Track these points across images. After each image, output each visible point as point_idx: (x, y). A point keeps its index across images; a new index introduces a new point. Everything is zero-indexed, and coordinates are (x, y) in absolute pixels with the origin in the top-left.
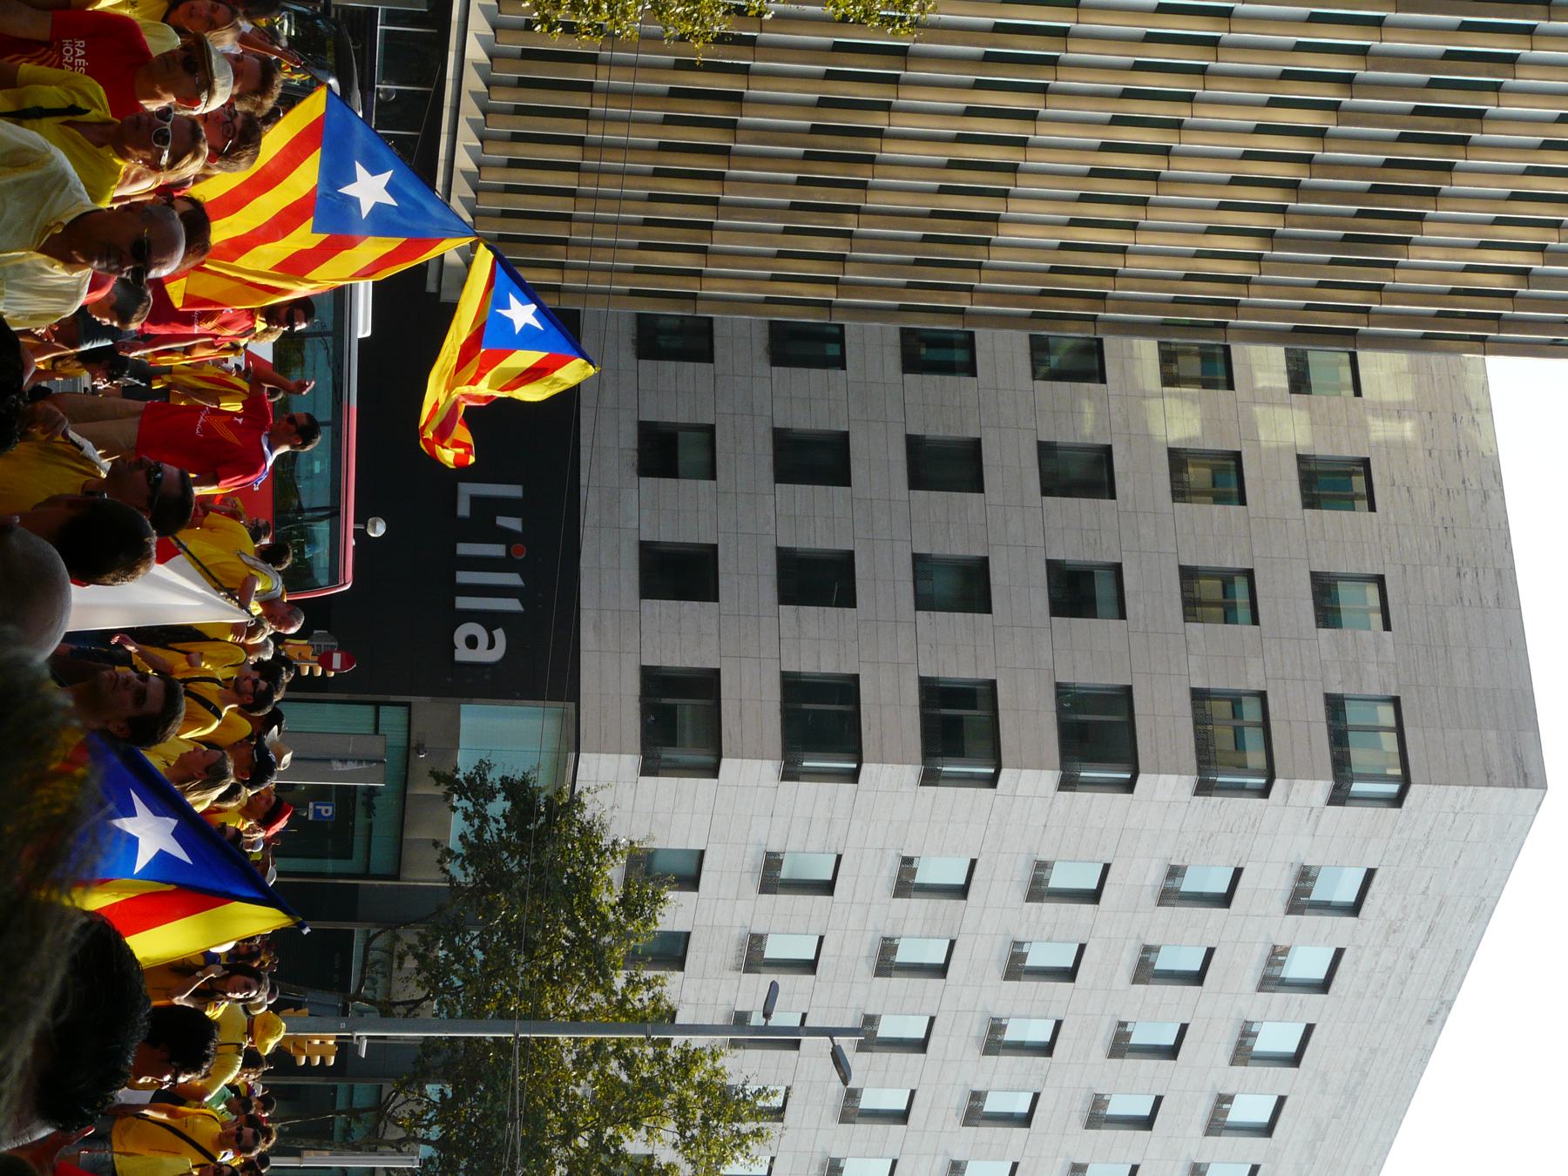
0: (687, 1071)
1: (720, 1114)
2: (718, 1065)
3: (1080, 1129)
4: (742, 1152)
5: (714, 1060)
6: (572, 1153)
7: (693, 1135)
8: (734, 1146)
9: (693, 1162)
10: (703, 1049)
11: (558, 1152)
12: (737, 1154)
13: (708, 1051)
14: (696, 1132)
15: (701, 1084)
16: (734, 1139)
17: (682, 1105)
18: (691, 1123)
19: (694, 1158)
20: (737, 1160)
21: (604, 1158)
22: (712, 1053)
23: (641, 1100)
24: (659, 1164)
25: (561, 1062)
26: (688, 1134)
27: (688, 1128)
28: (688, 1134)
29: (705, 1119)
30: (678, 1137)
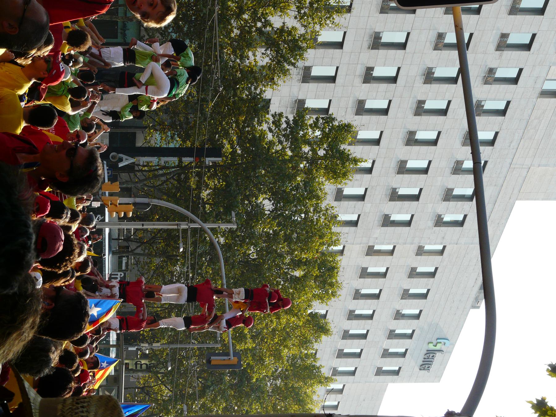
6: (242, 23)
7: (305, 12)
8: (326, 18)
9: (305, 26)
11: (234, 23)
12: (328, 22)
14: (306, 10)
16: (326, 14)
18: (304, 6)
19: (305, 24)
20: (328, 25)
21: (259, 24)
24: (288, 28)
26: (302, 12)
27: (302, 8)
30: (297, 13)
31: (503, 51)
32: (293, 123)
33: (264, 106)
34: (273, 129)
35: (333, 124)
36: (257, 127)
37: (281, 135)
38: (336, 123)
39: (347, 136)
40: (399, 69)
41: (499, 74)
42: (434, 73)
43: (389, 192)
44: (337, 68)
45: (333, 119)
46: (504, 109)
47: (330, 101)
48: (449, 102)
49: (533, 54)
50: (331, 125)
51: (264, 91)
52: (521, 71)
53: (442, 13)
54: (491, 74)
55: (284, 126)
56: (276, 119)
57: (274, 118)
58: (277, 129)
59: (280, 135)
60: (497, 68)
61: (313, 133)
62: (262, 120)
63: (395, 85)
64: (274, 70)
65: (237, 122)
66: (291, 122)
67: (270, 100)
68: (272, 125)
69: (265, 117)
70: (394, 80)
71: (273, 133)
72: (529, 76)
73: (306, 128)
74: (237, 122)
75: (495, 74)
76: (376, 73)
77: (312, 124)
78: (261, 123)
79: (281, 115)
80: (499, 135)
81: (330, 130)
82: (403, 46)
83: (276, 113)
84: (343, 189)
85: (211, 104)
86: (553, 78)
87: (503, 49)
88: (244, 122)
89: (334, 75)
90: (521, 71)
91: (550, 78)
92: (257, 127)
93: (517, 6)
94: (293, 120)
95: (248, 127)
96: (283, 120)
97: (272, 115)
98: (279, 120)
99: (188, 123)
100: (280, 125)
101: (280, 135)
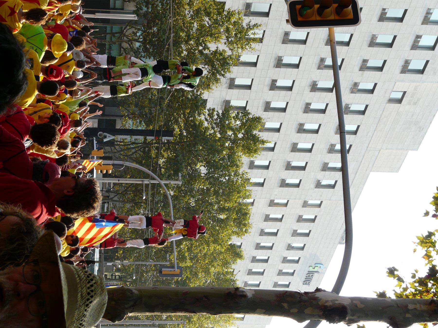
0: (230, 18)
1: (241, 32)
2: (240, 16)
3: (367, 47)
4: (249, 46)
5: (239, 15)
6: (189, 47)
8: (246, 44)
9: (232, 50)
10: (235, 11)
13: (237, 12)
15: (235, 22)
17: (227, 30)
18: (231, 36)
21: (201, 48)
22: (238, 12)
23: (214, 27)
24: (220, 51)
25: (185, 15)
26: (230, 40)
28: (230, 40)
29: (236, 35)
31: (364, 71)
32: (221, 115)
33: (202, 103)
34: (208, 119)
35: (248, 117)
36: (198, 117)
37: (214, 123)
38: (251, 116)
39: (258, 125)
40: (294, 81)
41: (361, 87)
42: (317, 85)
43: (285, 164)
44: (253, 80)
45: (249, 113)
46: (364, 110)
47: (247, 102)
48: (327, 105)
49: (384, 73)
50: (247, 117)
51: (203, 93)
52: (376, 84)
53: (324, 45)
54: (356, 86)
55: (216, 117)
56: (210, 112)
57: (209, 112)
58: (211, 119)
59: (213, 123)
60: (360, 83)
61: (235, 122)
62: (201, 113)
63: (291, 92)
64: (210, 79)
65: (184, 114)
66: (221, 115)
67: (207, 100)
68: (207, 116)
69: (203, 111)
70: (290, 89)
71: (208, 122)
72: (381, 89)
73: (230, 119)
74: (184, 114)
75: (358, 86)
76: (278, 84)
77: (234, 116)
78: (200, 115)
79: (213, 110)
80: (360, 128)
81: (246, 121)
82: (297, 66)
83: (210, 108)
84: (254, 161)
85: (167, 101)
86: (397, 91)
87: (364, 70)
88: (189, 114)
89: (250, 84)
90: (376, 84)
91: (395, 91)
92: (198, 117)
93: (374, 41)
94: (222, 114)
95: (191, 117)
96: (215, 113)
97: (208, 110)
98: (212, 113)
99: (151, 113)
100: (213, 117)
101: (213, 123)
